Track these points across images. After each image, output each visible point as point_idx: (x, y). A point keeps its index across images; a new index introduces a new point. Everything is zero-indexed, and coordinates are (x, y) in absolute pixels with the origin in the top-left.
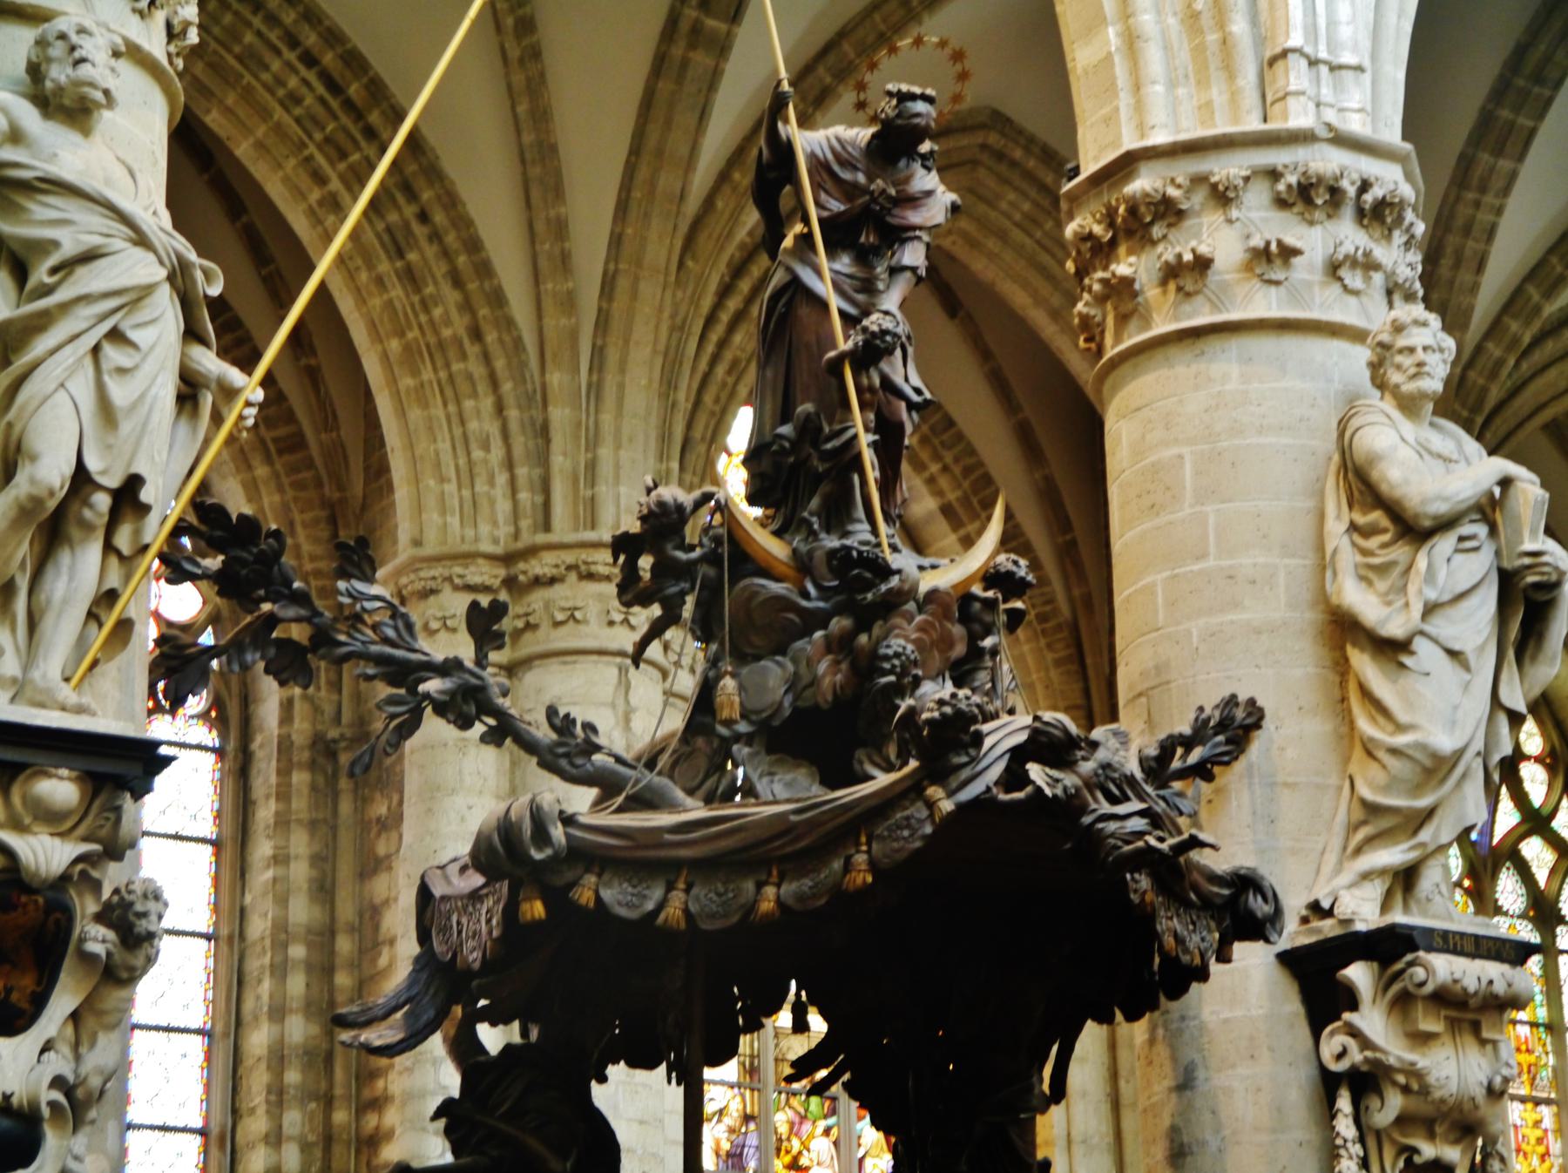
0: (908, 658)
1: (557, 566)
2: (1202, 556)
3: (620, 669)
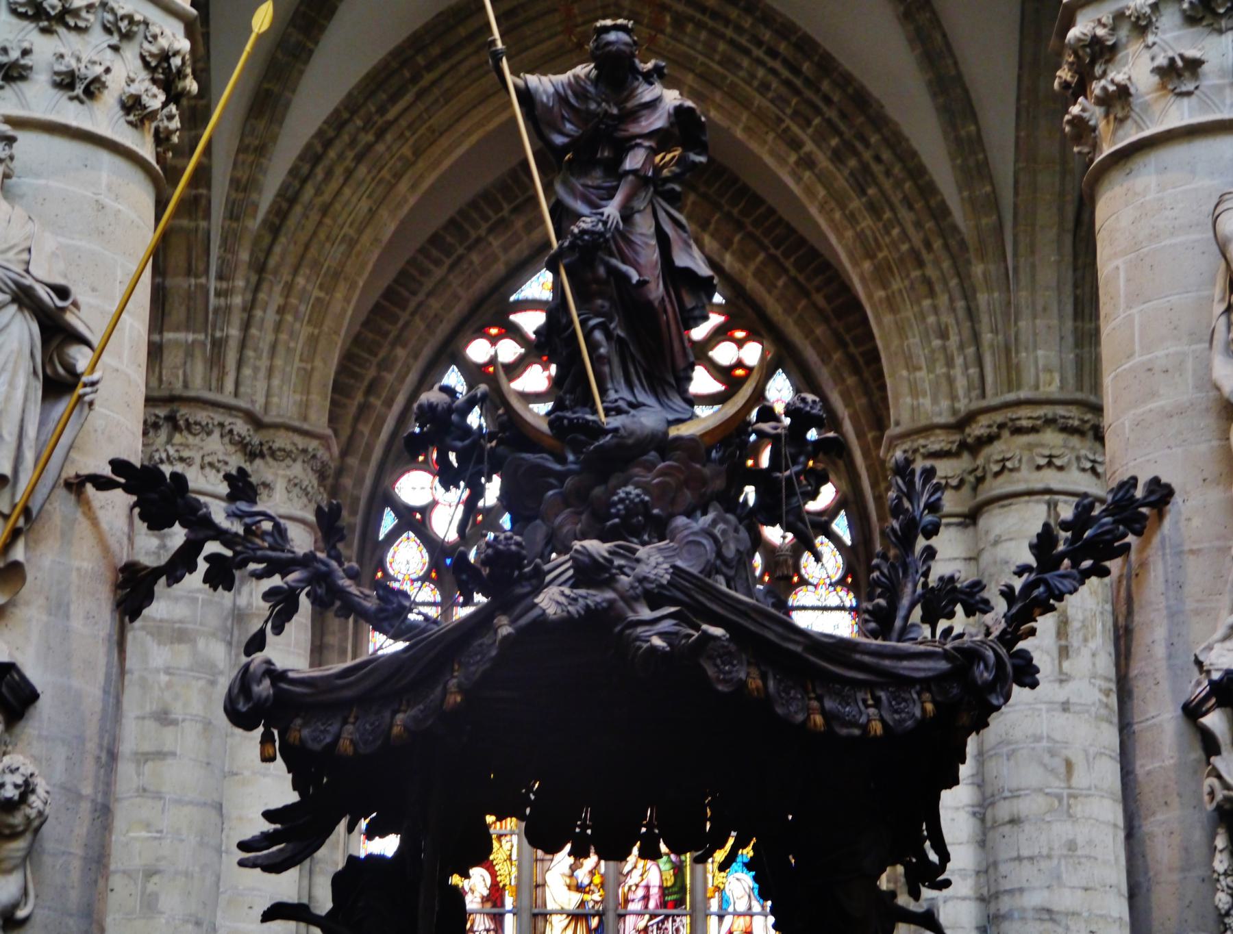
0: (632, 501)
1: (990, 426)
2: (1130, 356)
3: (1049, 504)
